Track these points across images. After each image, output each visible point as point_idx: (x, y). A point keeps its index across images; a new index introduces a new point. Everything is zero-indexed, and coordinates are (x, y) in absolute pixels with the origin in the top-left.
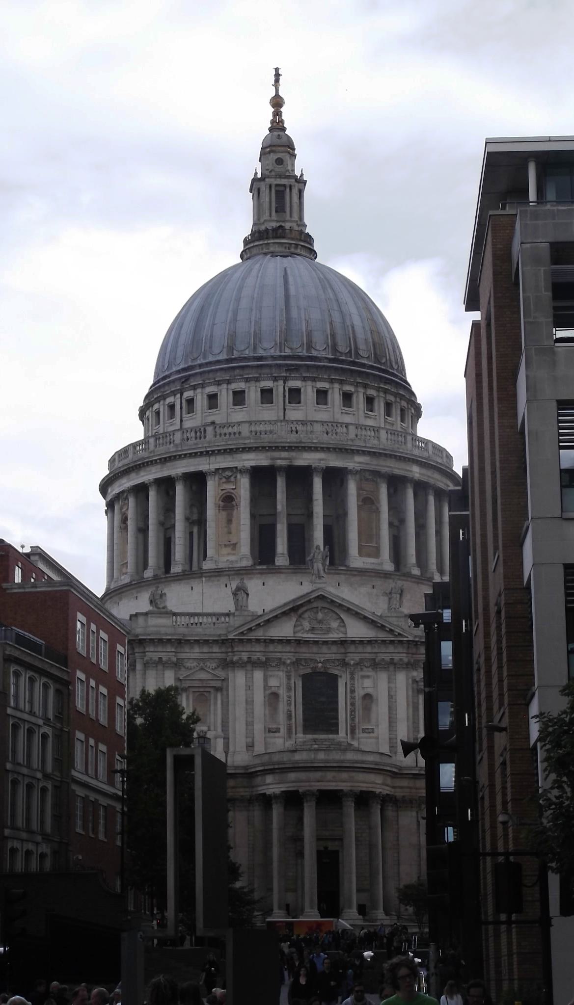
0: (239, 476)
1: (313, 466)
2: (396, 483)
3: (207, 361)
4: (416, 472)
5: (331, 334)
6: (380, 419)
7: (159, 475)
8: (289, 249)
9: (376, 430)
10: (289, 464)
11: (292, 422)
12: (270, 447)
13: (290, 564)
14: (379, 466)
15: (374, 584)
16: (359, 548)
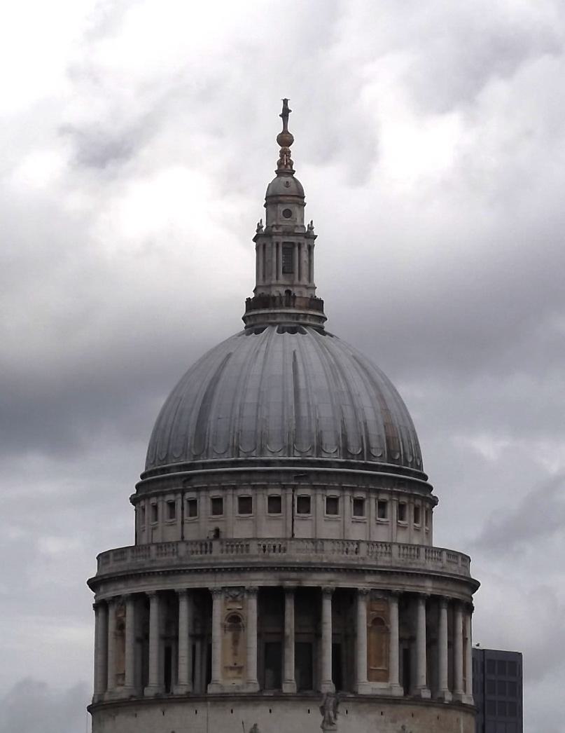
0: (246, 596)
1: (323, 588)
2: (407, 601)
3: (210, 460)
4: (428, 588)
5: (342, 435)
6: (392, 525)
7: (160, 588)
8: (297, 319)
9: (388, 545)
10: (298, 585)
11: (302, 540)
12: (279, 569)
13: (299, 689)
14: (392, 584)
15: (383, 710)
16: (368, 672)
